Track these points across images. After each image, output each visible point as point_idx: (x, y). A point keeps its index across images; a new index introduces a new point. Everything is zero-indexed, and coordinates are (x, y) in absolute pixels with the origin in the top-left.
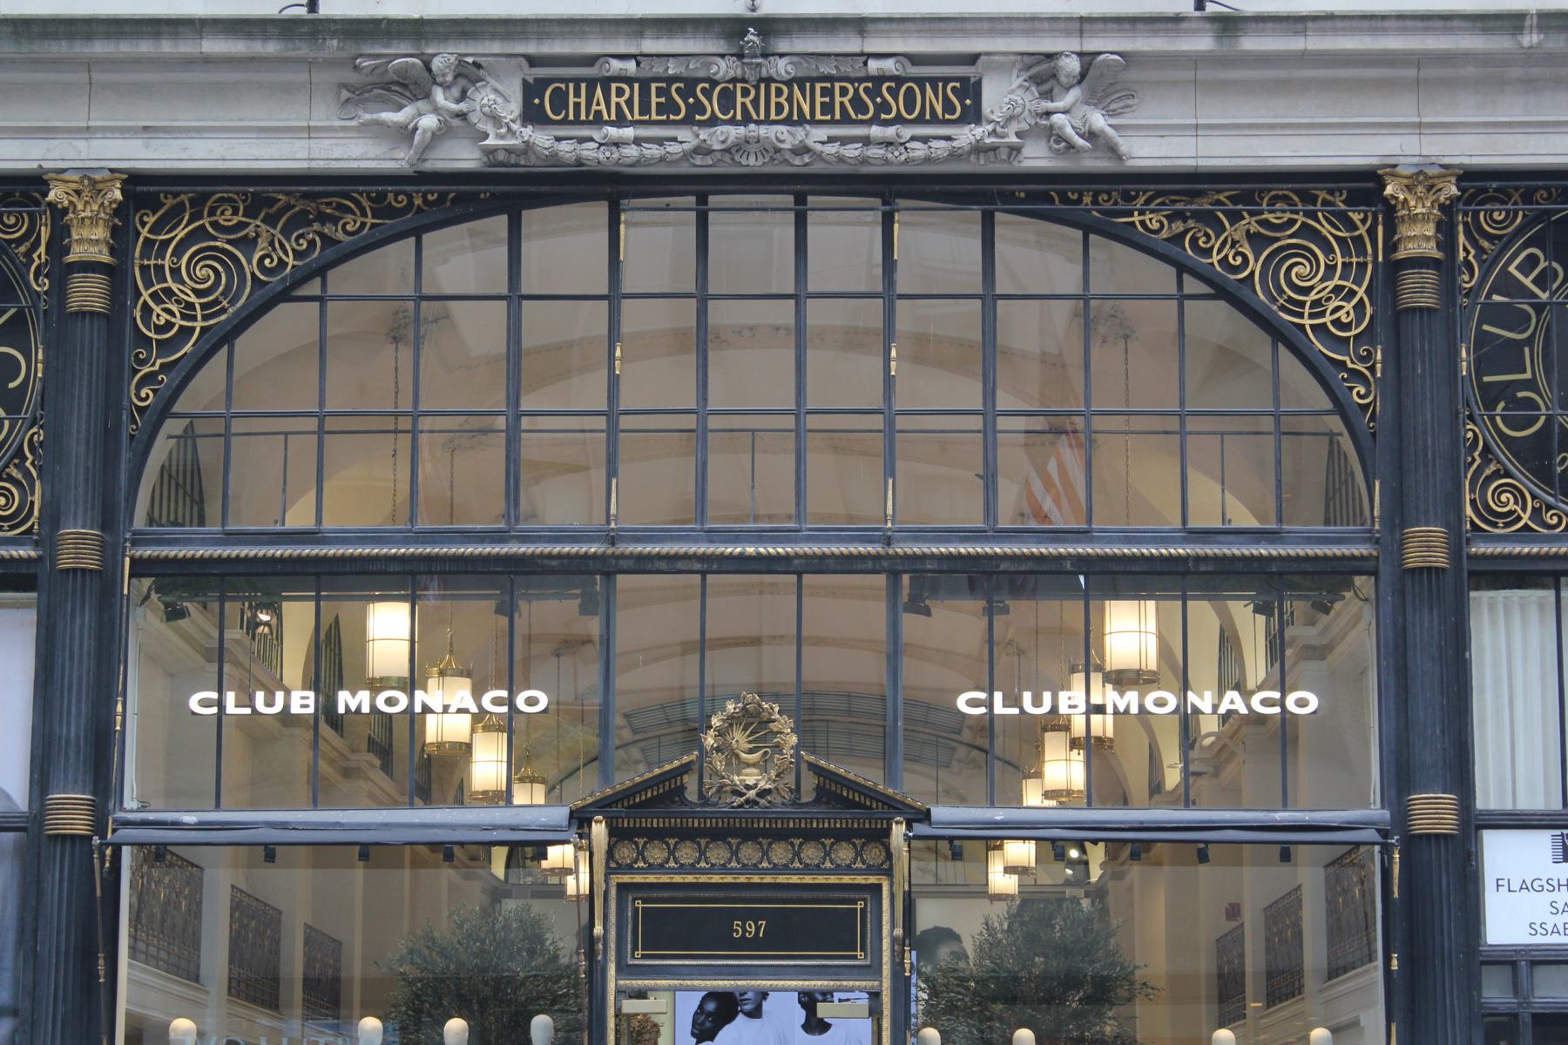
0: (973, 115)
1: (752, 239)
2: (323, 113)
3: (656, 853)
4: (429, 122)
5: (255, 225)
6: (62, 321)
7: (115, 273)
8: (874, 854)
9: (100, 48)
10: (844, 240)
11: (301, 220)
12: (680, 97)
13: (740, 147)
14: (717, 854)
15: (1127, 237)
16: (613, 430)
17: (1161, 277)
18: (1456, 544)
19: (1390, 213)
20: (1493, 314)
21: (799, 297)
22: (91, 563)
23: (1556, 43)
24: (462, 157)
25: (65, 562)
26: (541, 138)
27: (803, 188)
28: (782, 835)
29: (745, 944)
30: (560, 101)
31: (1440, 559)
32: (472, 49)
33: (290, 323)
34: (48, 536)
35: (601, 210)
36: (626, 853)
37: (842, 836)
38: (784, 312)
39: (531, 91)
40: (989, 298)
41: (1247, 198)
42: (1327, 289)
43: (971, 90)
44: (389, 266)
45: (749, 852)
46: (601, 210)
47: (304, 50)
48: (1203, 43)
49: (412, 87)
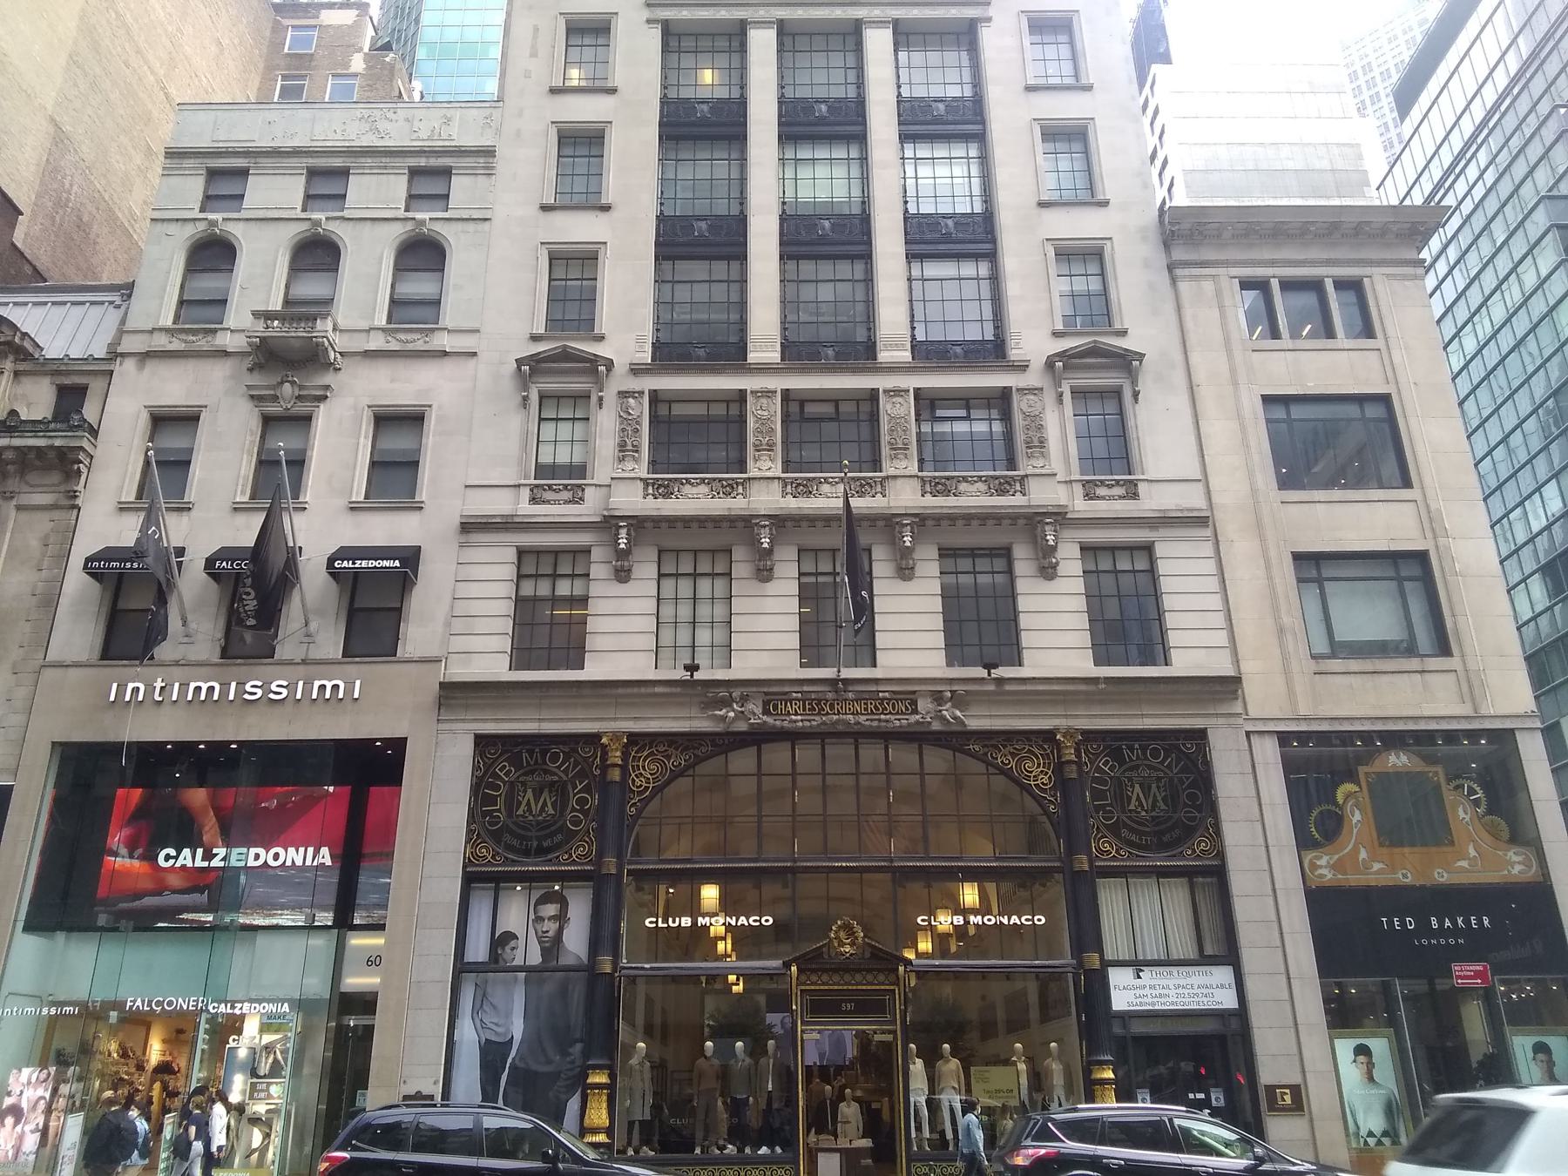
1: (840, 753)
2: (694, 712)
3: (814, 978)
4: (732, 714)
5: (671, 750)
6: (604, 786)
7: (624, 768)
8: (892, 977)
9: (620, 691)
10: (871, 754)
11: (686, 749)
12: (814, 704)
13: (838, 721)
14: (836, 978)
15: (968, 753)
16: (794, 821)
17: (981, 767)
18: (1091, 862)
19: (1058, 743)
20: (1095, 780)
21: (857, 774)
22: (613, 871)
24: (742, 727)
25: (604, 871)
26: (769, 720)
27: (858, 736)
28: (859, 971)
29: (846, 1012)
30: (775, 707)
31: (1086, 867)
32: (745, 690)
33: (683, 783)
34: (598, 862)
35: (788, 745)
36: (803, 978)
37: (879, 971)
38: (850, 781)
39: (766, 704)
40: (922, 775)
41: (1008, 740)
42: (1038, 773)
43: (914, 703)
44: (712, 766)
45: (847, 977)
46: (788, 745)
47: (690, 691)
48: (992, 687)
49: (726, 703)
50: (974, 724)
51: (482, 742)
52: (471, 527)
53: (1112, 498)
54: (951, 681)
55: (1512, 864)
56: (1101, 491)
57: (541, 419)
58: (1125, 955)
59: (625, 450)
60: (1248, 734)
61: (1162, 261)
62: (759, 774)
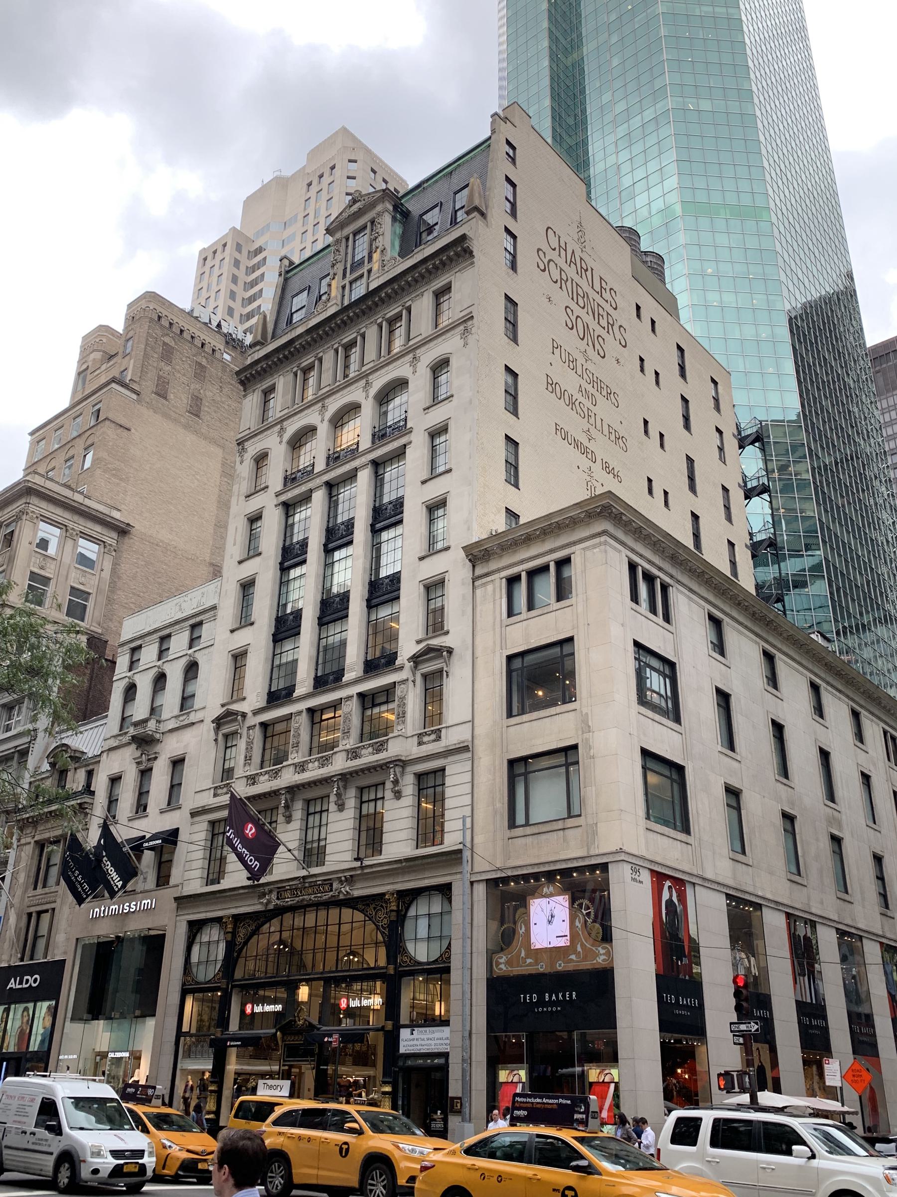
0: (331, 890)
12: (294, 891)
23: (408, 864)
24: (271, 907)
39: (278, 893)
41: (373, 900)
43: (331, 885)
49: (263, 895)
50: (356, 893)
51: (191, 923)
52: (194, 814)
53: (429, 742)
54: (343, 871)
55: (598, 955)
56: (426, 739)
57: (226, 748)
58: (407, 1022)
59: (248, 759)
60: (472, 883)
61: (470, 575)
62: (281, 931)
